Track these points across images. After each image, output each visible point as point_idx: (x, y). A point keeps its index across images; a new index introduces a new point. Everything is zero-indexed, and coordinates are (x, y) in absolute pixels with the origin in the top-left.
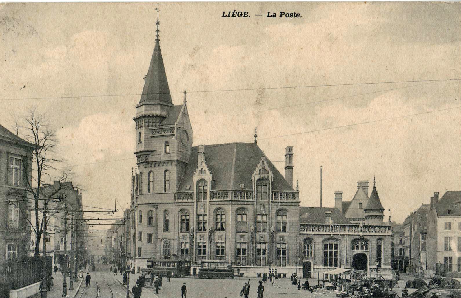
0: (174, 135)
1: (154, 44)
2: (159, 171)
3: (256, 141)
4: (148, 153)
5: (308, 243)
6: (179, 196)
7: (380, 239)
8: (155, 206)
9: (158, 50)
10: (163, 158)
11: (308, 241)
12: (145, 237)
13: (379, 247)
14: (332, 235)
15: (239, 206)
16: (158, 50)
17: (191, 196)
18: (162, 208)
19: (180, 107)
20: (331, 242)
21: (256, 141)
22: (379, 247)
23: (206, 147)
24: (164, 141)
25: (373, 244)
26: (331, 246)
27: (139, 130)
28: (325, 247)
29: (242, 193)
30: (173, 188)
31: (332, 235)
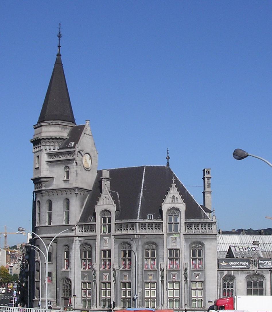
0: (74, 159)
3: (168, 164)
4: (45, 180)
5: (228, 281)
9: (59, 64)
10: (63, 186)
14: (255, 271)
15: (146, 240)
16: (59, 64)
20: (255, 279)
21: (168, 164)
24: (64, 166)
26: (255, 284)
27: (37, 154)
28: (249, 284)
29: (151, 225)
31: (255, 271)
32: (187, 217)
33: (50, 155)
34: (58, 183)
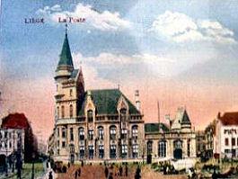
1: (64, 37)
2: (67, 106)
6: (78, 119)
7: (189, 140)
8: (66, 125)
9: (67, 40)
11: (150, 142)
12: (61, 144)
13: (189, 145)
16: (67, 40)
17: (84, 118)
18: (69, 127)
19: (77, 70)
22: (189, 145)
23: (92, 92)
25: (185, 142)
30: (75, 116)
32: (130, 113)
33: (63, 84)
34: (67, 97)
